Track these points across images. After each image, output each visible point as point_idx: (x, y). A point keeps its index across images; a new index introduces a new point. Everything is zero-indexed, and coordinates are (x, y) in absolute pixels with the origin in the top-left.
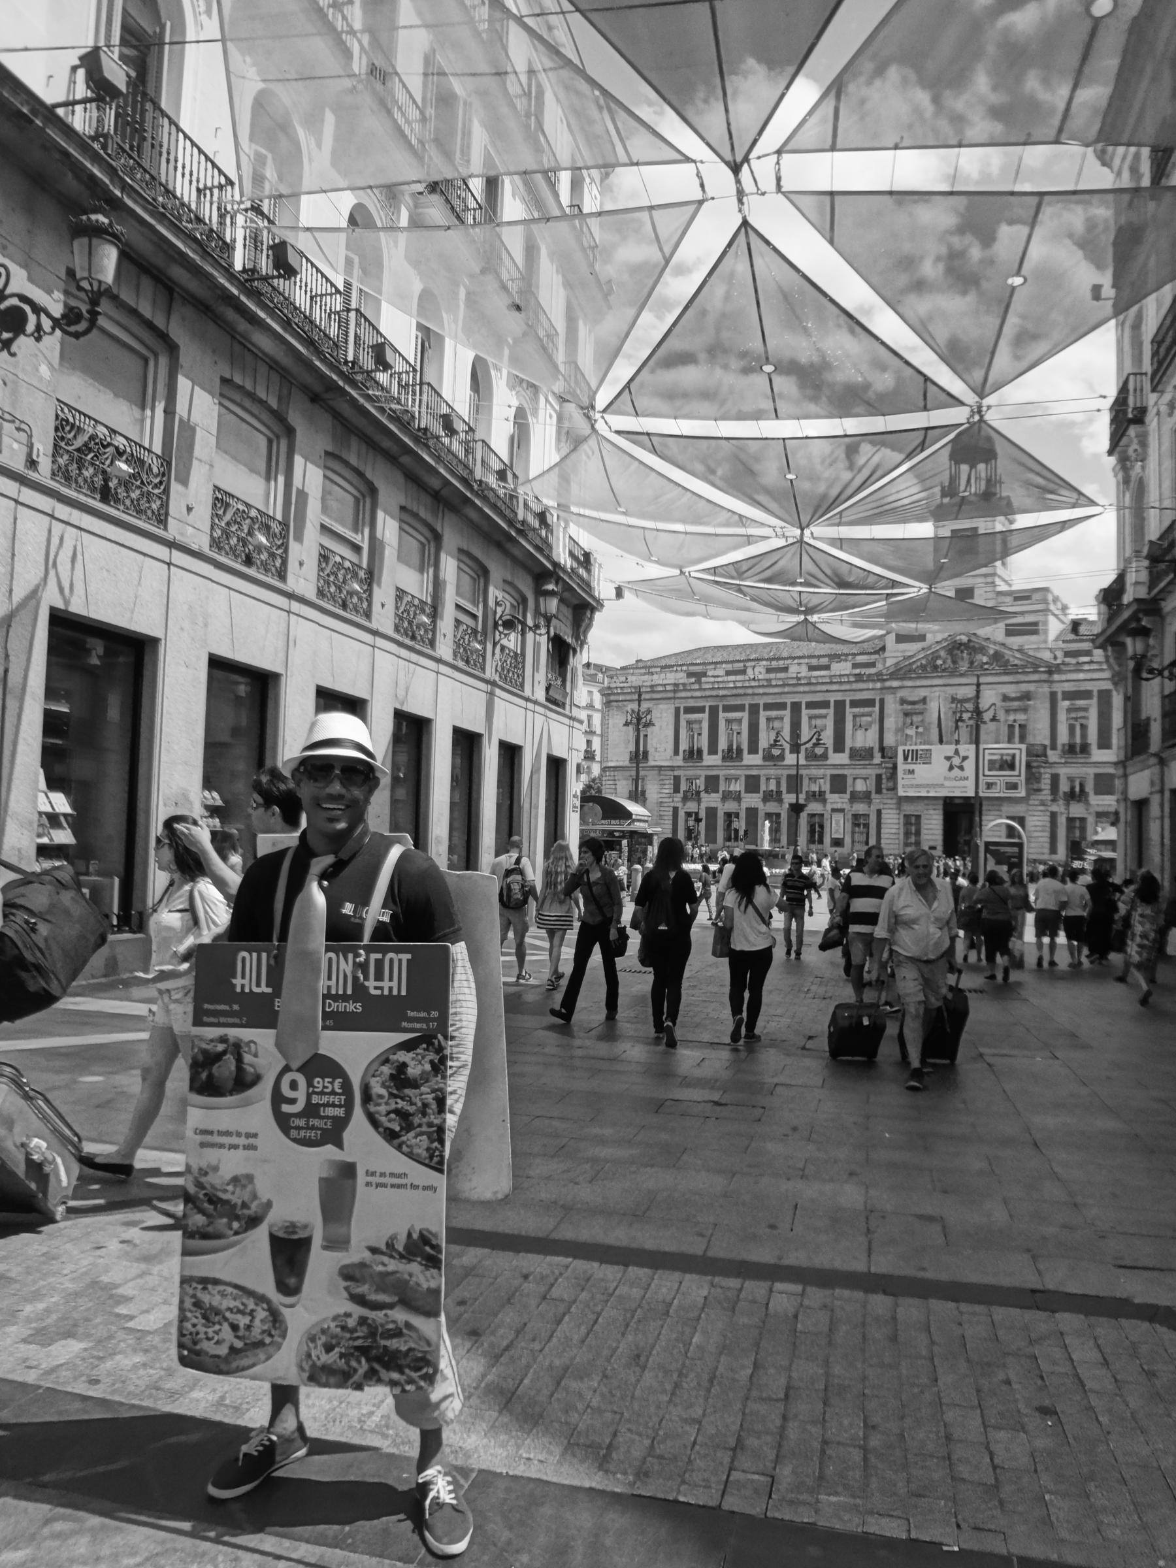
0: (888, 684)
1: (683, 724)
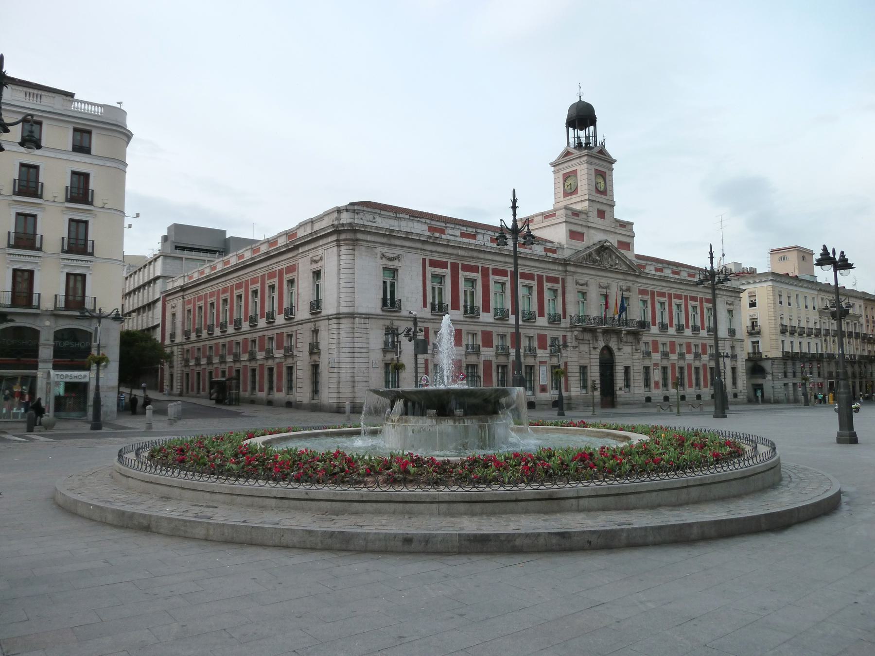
1: (429, 276)
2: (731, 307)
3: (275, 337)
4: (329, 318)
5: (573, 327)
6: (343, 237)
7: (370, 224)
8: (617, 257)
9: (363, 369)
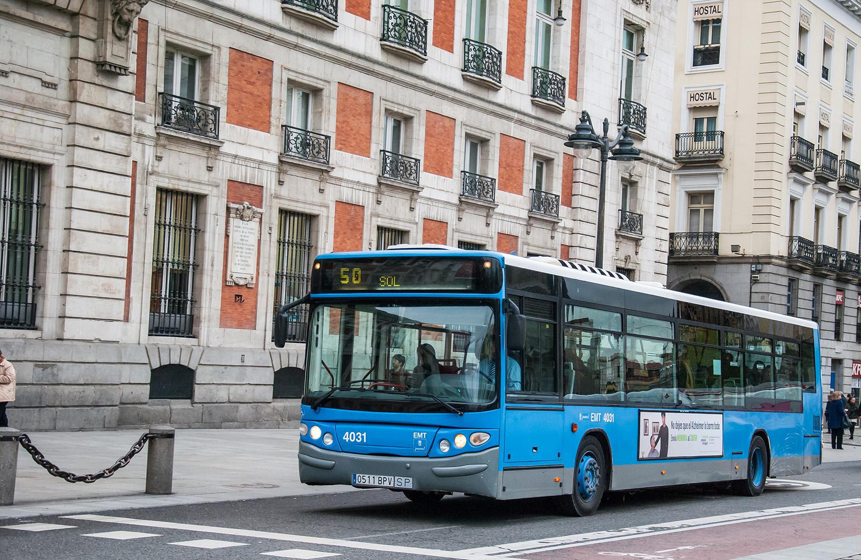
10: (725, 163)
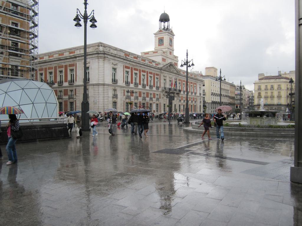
0: (162, 71)
2: (200, 86)
3: (63, 91)
4: (94, 85)
5: (163, 91)
6: (100, 55)
7: (109, 51)
8: (174, 68)
9: (107, 104)
10: (206, 95)
